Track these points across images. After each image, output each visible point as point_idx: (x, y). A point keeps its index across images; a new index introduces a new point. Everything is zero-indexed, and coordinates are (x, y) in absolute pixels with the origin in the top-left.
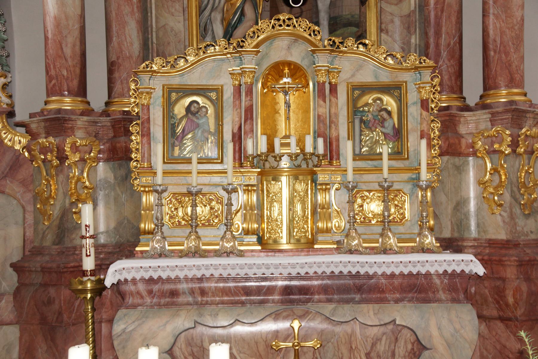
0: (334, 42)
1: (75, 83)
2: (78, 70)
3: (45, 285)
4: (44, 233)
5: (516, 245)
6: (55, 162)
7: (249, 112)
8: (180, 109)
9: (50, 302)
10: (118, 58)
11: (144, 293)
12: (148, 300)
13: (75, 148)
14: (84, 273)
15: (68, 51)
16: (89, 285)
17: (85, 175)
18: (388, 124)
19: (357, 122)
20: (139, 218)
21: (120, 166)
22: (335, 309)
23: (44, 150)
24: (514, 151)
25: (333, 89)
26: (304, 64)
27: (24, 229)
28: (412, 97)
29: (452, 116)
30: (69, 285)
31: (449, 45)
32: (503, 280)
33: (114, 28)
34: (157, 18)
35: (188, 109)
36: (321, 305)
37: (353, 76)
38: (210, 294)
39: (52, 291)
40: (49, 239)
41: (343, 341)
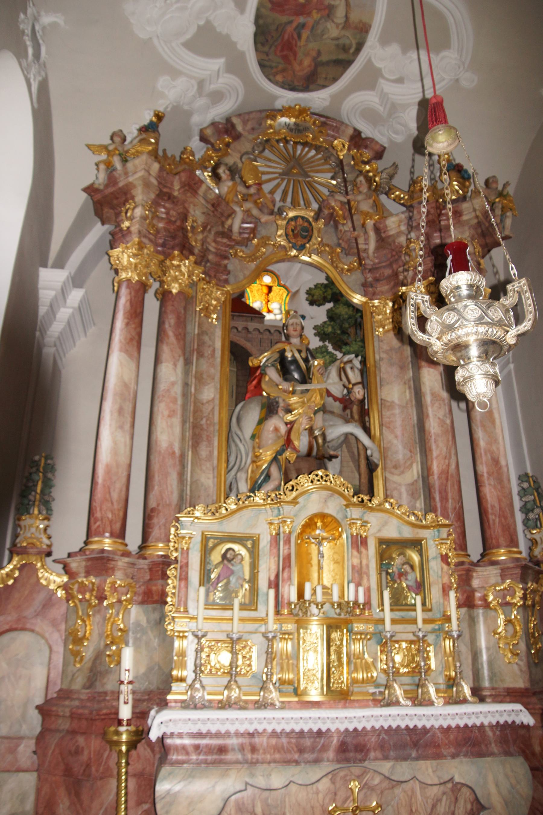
0: (362, 499)
1: (117, 526)
2: (121, 514)
3: (73, 732)
4: (73, 675)
6: (95, 602)
7: (288, 558)
9: (78, 752)
10: (158, 505)
11: (190, 749)
12: (194, 757)
14: (120, 723)
15: (115, 495)
16: (124, 737)
17: (121, 617)
19: (384, 574)
21: (154, 610)
22: (393, 767)
25: (364, 542)
26: (339, 517)
27: (49, 669)
31: (455, 508)
33: (157, 478)
34: (192, 473)
35: (224, 556)
36: (378, 763)
37: (379, 531)
38: (261, 751)
39: (81, 740)
41: (404, 803)
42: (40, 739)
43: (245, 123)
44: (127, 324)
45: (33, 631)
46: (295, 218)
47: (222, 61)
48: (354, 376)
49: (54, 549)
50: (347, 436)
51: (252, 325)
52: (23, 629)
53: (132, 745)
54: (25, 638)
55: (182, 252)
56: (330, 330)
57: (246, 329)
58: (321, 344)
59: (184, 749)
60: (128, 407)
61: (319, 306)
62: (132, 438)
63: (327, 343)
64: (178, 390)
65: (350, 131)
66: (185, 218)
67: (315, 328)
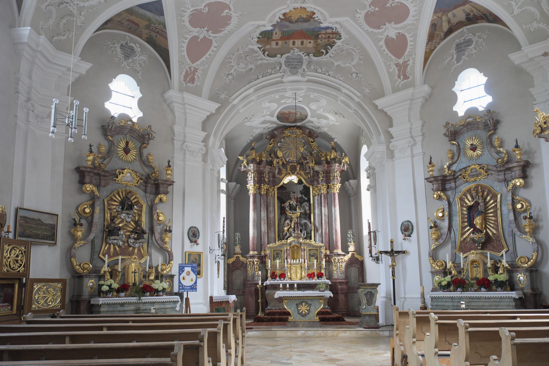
6: (252, 264)
8: (275, 253)
18: (316, 256)
23: (249, 262)
35: (277, 253)
43: (278, 132)
44: (253, 205)
45: (240, 270)
46: (292, 165)
47: (270, 124)
48: (307, 208)
51: (284, 191)
52: (238, 269)
54: (239, 271)
56: (303, 192)
57: (282, 193)
58: (301, 196)
61: (301, 184)
63: (303, 195)
64: (266, 218)
65: (308, 131)
67: (300, 191)
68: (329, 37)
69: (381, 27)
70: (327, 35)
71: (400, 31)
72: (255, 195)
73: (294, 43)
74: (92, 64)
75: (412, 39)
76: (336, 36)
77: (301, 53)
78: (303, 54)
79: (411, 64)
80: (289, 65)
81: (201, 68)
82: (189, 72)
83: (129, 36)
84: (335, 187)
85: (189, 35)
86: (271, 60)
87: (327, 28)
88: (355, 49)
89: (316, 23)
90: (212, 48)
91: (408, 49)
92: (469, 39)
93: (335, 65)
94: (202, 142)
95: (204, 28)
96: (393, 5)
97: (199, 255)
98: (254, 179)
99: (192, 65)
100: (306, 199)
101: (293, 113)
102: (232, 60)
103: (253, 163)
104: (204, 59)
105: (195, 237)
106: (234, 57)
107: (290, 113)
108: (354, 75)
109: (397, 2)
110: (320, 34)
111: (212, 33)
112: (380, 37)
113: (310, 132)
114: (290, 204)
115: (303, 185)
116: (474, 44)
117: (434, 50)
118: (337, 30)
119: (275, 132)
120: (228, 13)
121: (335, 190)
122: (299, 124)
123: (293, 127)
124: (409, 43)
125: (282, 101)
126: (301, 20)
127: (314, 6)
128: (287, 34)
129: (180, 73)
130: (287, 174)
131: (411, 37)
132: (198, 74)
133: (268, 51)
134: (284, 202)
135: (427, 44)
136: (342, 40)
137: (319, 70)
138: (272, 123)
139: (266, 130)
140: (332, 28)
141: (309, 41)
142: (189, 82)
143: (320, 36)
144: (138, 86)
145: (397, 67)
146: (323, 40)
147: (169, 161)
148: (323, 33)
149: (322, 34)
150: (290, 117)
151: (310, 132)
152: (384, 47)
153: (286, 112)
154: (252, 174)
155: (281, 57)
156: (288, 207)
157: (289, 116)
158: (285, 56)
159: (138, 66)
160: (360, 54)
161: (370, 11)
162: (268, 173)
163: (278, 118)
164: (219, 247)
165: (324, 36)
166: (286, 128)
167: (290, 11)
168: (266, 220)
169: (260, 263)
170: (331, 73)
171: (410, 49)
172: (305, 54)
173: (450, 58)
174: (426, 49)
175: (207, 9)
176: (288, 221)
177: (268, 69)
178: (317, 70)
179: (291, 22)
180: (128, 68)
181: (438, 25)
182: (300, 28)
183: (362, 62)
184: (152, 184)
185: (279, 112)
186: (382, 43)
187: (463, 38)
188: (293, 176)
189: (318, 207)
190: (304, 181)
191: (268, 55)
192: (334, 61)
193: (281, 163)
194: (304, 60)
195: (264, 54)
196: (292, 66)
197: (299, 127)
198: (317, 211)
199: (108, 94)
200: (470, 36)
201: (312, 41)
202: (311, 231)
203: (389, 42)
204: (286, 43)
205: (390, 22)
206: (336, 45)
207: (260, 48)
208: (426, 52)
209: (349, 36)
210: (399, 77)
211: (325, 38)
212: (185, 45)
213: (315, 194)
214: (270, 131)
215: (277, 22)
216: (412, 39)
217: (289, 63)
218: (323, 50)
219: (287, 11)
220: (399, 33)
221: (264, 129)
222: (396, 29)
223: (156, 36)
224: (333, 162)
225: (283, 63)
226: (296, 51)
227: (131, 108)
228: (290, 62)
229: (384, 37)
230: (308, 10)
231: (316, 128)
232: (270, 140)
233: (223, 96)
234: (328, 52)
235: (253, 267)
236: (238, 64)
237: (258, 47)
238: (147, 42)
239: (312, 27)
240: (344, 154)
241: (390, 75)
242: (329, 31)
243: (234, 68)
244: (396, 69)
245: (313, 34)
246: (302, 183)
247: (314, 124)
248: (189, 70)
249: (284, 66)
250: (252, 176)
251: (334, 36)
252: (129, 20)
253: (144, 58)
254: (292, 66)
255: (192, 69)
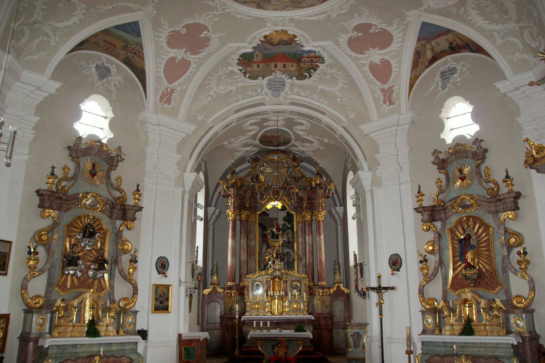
1: (234, 279)
5: (323, 314)
7: (269, 286)
13: (234, 293)
18: (298, 288)
20: (246, 308)
23: (227, 293)
24: (323, 295)
25: (287, 281)
26: (281, 276)
28: (303, 283)
29: (311, 287)
30: (233, 321)
32: (320, 321)
33: (241, 267)
39: (229, 322)
40: (228, 311)
42: (221, 323)
43: (261, 156)
48: (290, 236)
49: (220, 283)
50: (288, 252)
51: (265, 218)
53: (239, 323)
55: (244, 210)
56: (287, 218)
57: (264, 219)
59: (248, 323)
60: (234, 252)
62: (235, 259)
64: (245, 246)
65: (292, 155)
66: (244, 198)
67: (283, 218)
68: (312, 61)
69: (365, 52)
70: (310, 59)
71: (385, 57)
72: (234, 221)
73: (276, 66)
74: (62, 84)
75: (397, 65)
76: (319, 60)
77: (283, 76)
78: (286, 77)
79: (396, 90)
80: (271, 88)
81: (179, 88)
82: (166, 93)
83: (105, 57)
84: (320, 214)
85: (167, 56)
86: (253, 83)
87: (310, 51)
88: (339, 73)
89: (299, 46)
90: (191, 69)
91: (393, 75)
92: (453, 67)
93: (319, 89)
94: (176, 165)
95: (182, 49)
96: (376, 31)
97: (167, 287)
98: (234, 205)
99: (169, 86)
100: (289, 226)
101: (276, 136)
102: (212, 82)
103: (233, 187)
104: (182, 79)
105: (164, 268)
106: (214, 78)
107: (273, 137)
108: (339, 100)
109: (381, 29)
110: (303, 57)
111: (190, 54)
112: (364, 62)
113: (294, 156)
114: (272, 231)
115: (287, 211)
116: (458, 72)
117: (419, 77)
118: (320, 54)
119: (258, 156)
120: (206, 34)
121: (320, 217)
122: (282, 148)
123: (277, 150)
124: (394, 69)
125: (265, 124)
126: (282, 43)
127: (295, 30)
128: (268, 57)
129: (156, 94)
130: (271, 200)
131: (395, 63)
132: (175, 95)
133: (250, 74)
134: (266, 230)
135: (412, 71)
136: (325, 64)
137: (303, 94)
138: (255, 146)
139: (248, 153)
140: (315, 52)
141: (291, 64)
142: (165, 103)
143: (303, 59)
144: (111, 106)
145: (382, 92)
146: (306, 64)
147: (138, 184)
148: (305, 56)
149: (305, 57)
150: (274, 140)
151: (294, 156)
152: (369, 73)
153: (269, 135)
154: (232, 199)
155: (263, 79)
156: (269, 234)
157: (272, 140)
158: (267, 79)
159: (113, 87)
160: (345, 78)
161: (353, 36)
162: (250, 198)
163: (261, 141)
164: (193, 277)
165: (307, 60)
166: (270, 152)
167: (271, 34)
168: (246, 249)
169: (238, 295)
170: (315, 96)
171: (395, 75)
172: (288, 77)
173: (435, 85)
174: (411, 75)
175: (185, 30)
176: (269, 250)
177: (250, 92)
178: (300, 94)
179: (272, 44)
180: (102, 88)
181: (422, 53)
182: (282, 51)
183: (346, 87)
184: (118, 210)
185: (261, 135)
186: (367, 68)
187: (447, 66)
188: (277, 202)
189: (301, 235)
190: (287, 207)
191: (249, 77)
192: (318, 85)
193: (263, 188)
194: (287, 83)
195: (245, 76)
196: (274, 89)
197: (283, 152)
198: (300, 240)
199: (77, 115)
200: (454, 64)
201: (295, 65)
202: (294, 261)
203: (373, 67)
204: (267, 65)
205: (373, 48)
206: (320, 68)
207: (241, 70)
208: (411, 79)
209: (332, 61)
210: (385, 102)
211: (308, 62)
212: (163, 66)
213: (299, 221)
214: (253, 155)
215: (258, 45)
216: (397, 65)
217: (271, 86)
218: (305, 74)
219: (267, 33)
220: (383, 59)
221: (247, 152)
222: (380, 55)
223: (133, 57)
224: (318, 187)
225: (265, 85)
226: (278, 74)
227: (102, 129)
228: (272, 85)
229: (368, 62)
230: (290, 32)
231: (300, 152)
232: (252, 164)
233: (200, 118)
234: (311, 76)
235: (231, 299)
236: (218, 86)
237: (239, 69)
238: (123, 63)
239: (294, 50)
240: (329, 179)
241: (376, 100)
242: (312, 55)
243: (213, 90)
244: (381, 94)
245: (295, 57)
246: (286, 209)
247: (298, 148)
248: (165, 91)
249: (266, 89)
250: (233, 201)
251: (317, 60)
252: (106, 41)
253: (120, 78)
254: (274, 89)
255: (169, 90)
